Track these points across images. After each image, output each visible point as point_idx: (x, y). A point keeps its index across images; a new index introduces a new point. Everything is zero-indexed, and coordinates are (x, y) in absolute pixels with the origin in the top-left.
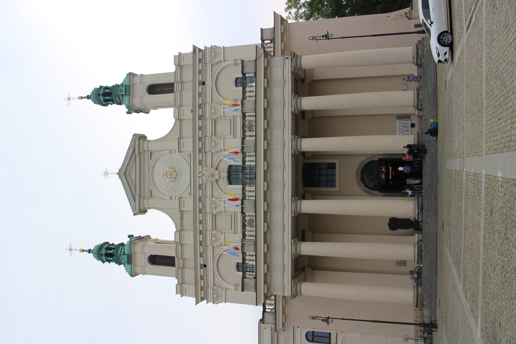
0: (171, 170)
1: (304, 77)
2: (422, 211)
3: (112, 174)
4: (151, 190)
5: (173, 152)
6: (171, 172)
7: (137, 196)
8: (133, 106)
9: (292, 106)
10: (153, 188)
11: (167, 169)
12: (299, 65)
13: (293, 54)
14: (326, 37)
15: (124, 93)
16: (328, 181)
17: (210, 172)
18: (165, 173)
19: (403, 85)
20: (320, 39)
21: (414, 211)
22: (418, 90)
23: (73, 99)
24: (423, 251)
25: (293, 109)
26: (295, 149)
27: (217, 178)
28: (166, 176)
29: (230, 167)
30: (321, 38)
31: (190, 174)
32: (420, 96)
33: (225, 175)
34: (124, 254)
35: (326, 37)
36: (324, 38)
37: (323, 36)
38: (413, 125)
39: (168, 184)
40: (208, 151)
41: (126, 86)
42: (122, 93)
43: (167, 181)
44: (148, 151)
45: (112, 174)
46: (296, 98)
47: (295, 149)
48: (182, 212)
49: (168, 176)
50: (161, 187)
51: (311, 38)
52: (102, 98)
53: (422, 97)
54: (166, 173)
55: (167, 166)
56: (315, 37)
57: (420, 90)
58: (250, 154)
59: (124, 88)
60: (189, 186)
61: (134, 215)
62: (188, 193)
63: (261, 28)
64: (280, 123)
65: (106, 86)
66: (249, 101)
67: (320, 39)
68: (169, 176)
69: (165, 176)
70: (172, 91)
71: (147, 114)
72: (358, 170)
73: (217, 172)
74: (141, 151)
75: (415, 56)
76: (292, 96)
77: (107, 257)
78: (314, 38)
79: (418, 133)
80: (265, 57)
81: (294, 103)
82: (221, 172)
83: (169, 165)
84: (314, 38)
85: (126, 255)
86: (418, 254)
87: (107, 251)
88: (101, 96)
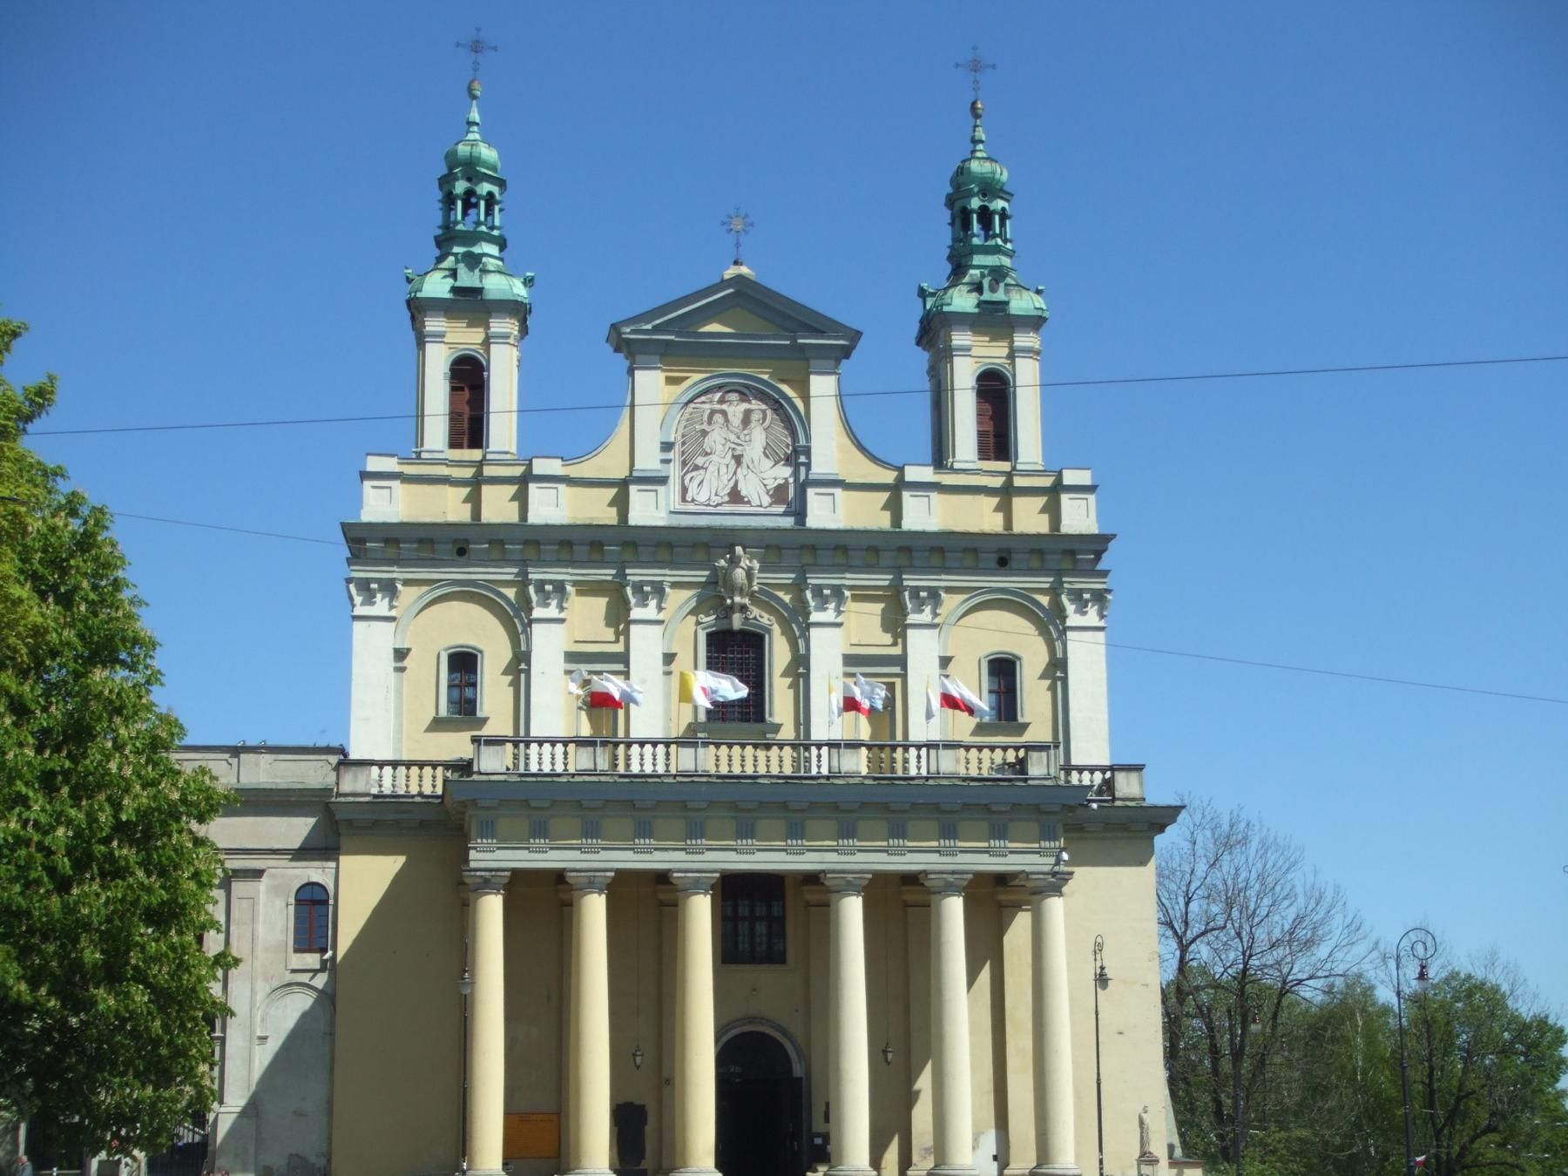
1: (1011, 884)
3: (738, 245)
4: (688, 378)
10: (695, 384)
13: (1067, 877)
14: (1102, 980)
15: (987, 296)
20: (1095, 960)
23: (976, 82)
30: (1099, 964)
33: (737, 621)
34: (484, 271)
35: (1102, 980)
36: (1098, 971)
37: (1102, 968)
41: (1007, 303)
45: (738, 245)
48: (623, 485)
51: (1099, 940)
52: (975, 203)
56: (1101, 950)
59: (1000, 296)
61: (613, 326)
63: (1144, 765)
67: (1095, 960)
70: (984, 454)
71: (914, 341)
76: (966, 873)
77: (464, 197)
78: (1098, 948)
84: (1098, 948)
85: (481, 281)
87: (482, 199)
88: (982, 203)
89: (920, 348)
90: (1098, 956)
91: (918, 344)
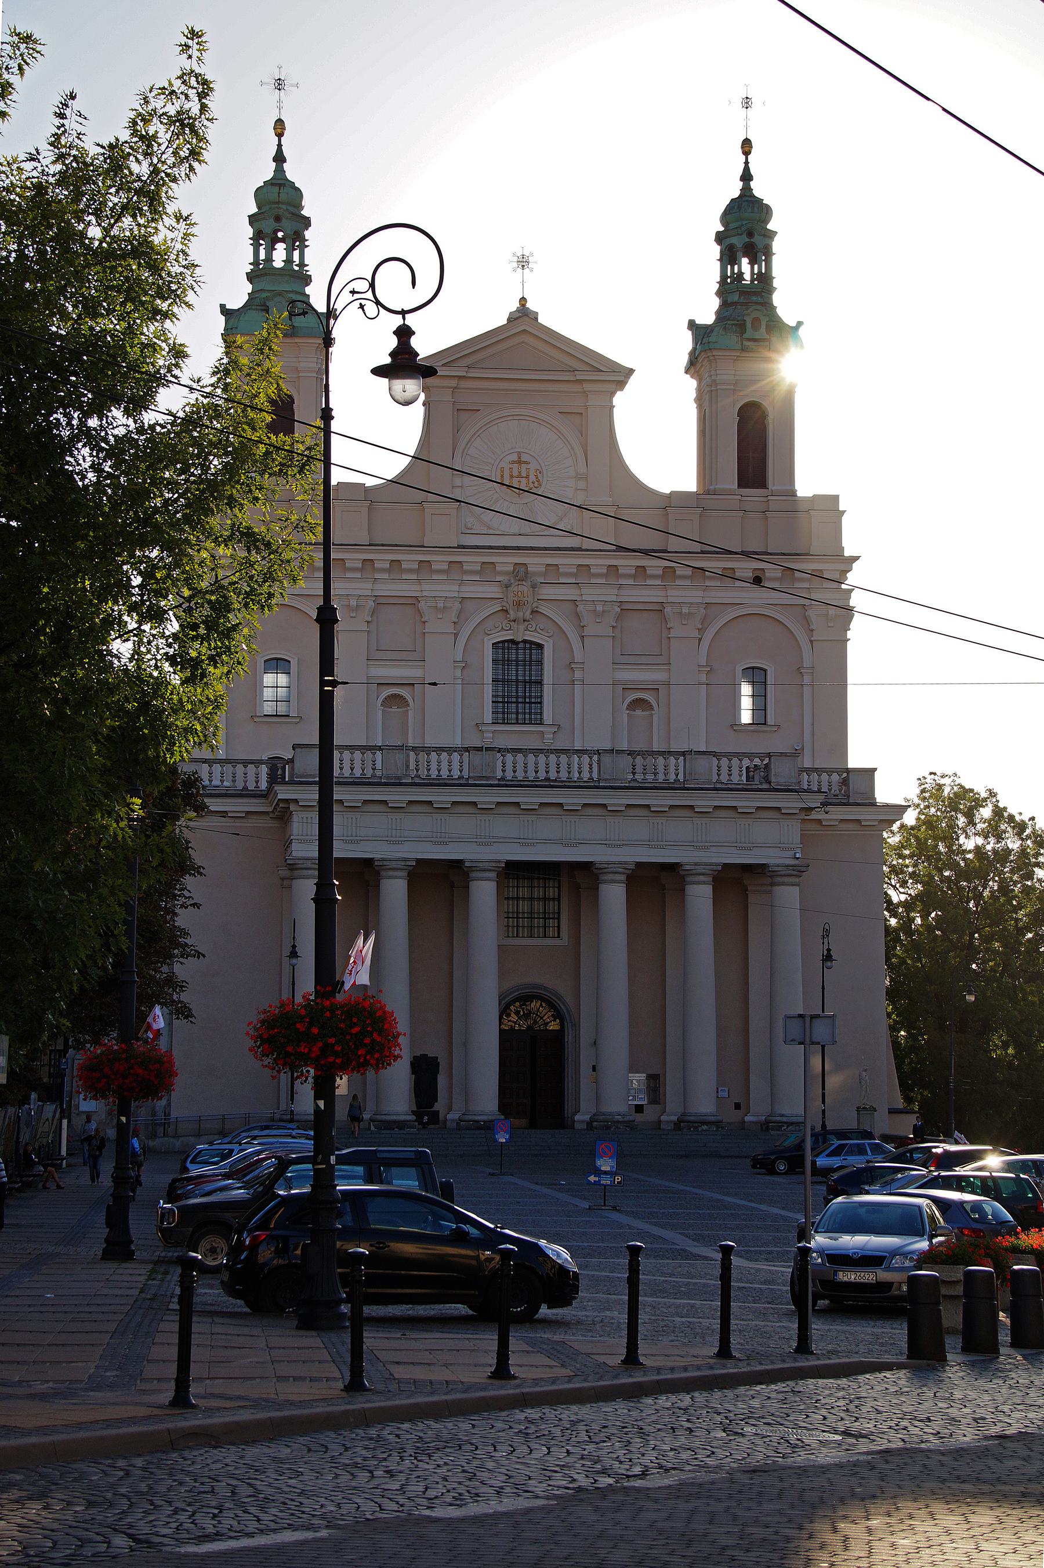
0: (532, 478)
2: (480, 1128)
5: (581, 485)
6: (527, 477)
7: (464, 374)
8: (711, 358)
9: (696, 864)
11: (533, 466)
12: (779, 879)
13: (803, 869)
14: (828, 957)
16: (518, 918)
17: (526, 599)
18: (524, 458)
19: (727, 1089)
21: (480, 1113)
22: (717, 1124)
24: (402, 1132)
25: (688, 867)
26: (606, 870)
27: (512, 615)
28: (514, 462)
29: (540, 647)
31: (521, 533)
32: (705, 1127)
35: (828, 957)
36: (825, 953)
37: (829, 950)
38: (639, 1109)
39: (495, 468)
40: (583, 591)
42: (749, 325)
43: (500, 466)
44: (586, 407)
46: (710, 872)
47: (606, 870)
49: (515, 466)
50: (484, 442)
51: (827, 927)
53: (703, 1130)
54: (525, 463)
55: (543, 465)
57: (718, 1127)
58: (595, 766)
60: (489, 528)
62: (469, 525)
64: (660, 839)
65: (774, 252)
66: (711, 768)
68: (515, 474)
69: (515, 457)
71: (683, 370)
72: (545, 989)
73: (528, 615)
74: (587, 387)
75: (784, 1119)
76: (717, 865)
78: (826, 933)
79: (633, 1121)
80: (802, 809)
81: (700, 869)
82: (526, 623)
83: (545, 472)
84: (826, 933)
86: (395, 1122)
89: (688, 376)
90: (826, 940)
91: (686, 372)
